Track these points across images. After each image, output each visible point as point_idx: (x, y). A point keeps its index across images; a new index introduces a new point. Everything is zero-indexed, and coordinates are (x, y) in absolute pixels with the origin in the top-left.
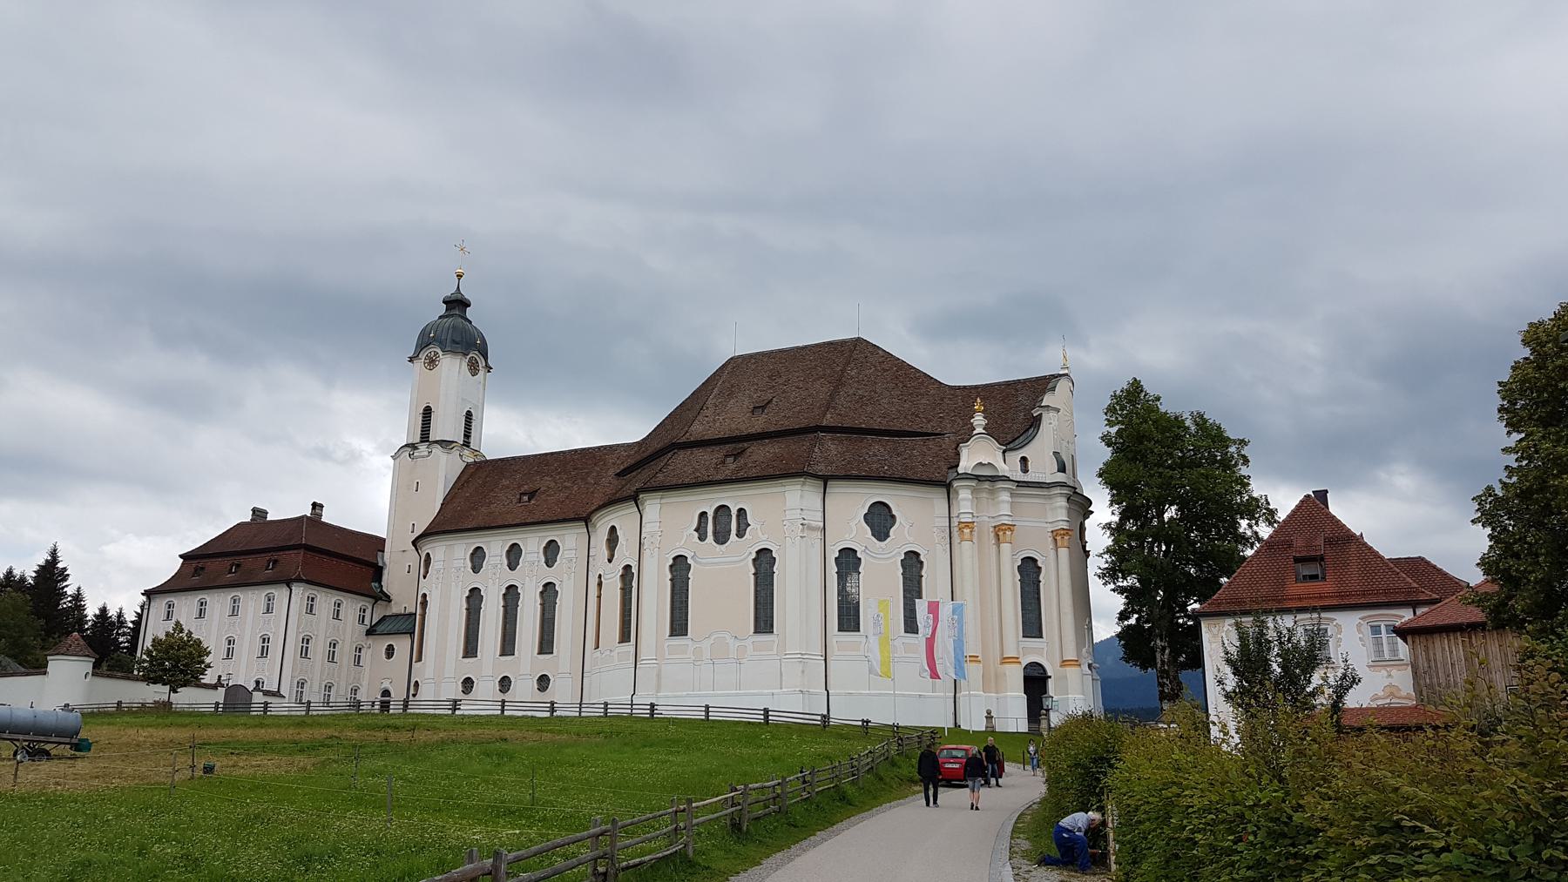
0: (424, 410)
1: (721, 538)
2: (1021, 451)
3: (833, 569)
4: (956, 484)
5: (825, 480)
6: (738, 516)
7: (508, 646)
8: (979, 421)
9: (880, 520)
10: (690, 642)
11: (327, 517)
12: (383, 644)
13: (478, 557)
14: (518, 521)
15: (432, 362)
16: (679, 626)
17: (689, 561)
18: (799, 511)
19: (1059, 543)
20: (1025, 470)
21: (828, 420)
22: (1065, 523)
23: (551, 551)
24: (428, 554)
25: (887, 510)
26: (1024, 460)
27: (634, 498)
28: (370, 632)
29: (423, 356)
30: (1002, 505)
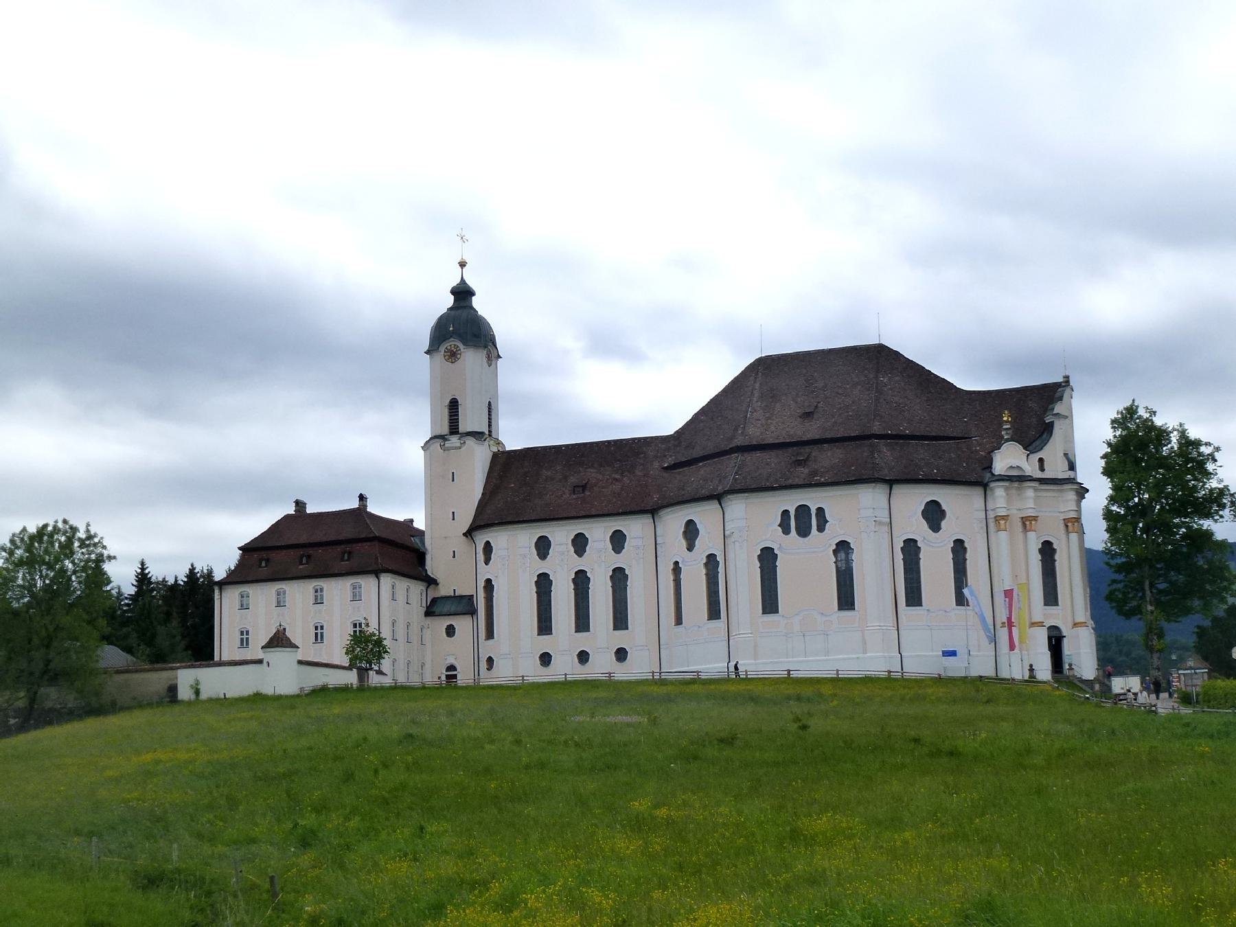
0: (450, 402)
1: (804, 531)
2: (1039, 453)
3: (899, 556)
4: (992, 485)
5: (891, 483)
6: (817, 515)
7: (582, 623)
9: (934, 515)
11: (373, 508)
12: (443, 623)
13: (543, 547)
14: (583, 513)
15: (453, 356)
16: (770, 604)
18: (872, 510)
19: (1070, 529)
20: (1042, 469)
21: (877, 428)
22: (1074, 513)
23: (618, 540)
24: (488, 544)
26: (1041, 460)
27: (718, 497)
28: (429, 613)
29: (442, 348)
30: (1029, 500)
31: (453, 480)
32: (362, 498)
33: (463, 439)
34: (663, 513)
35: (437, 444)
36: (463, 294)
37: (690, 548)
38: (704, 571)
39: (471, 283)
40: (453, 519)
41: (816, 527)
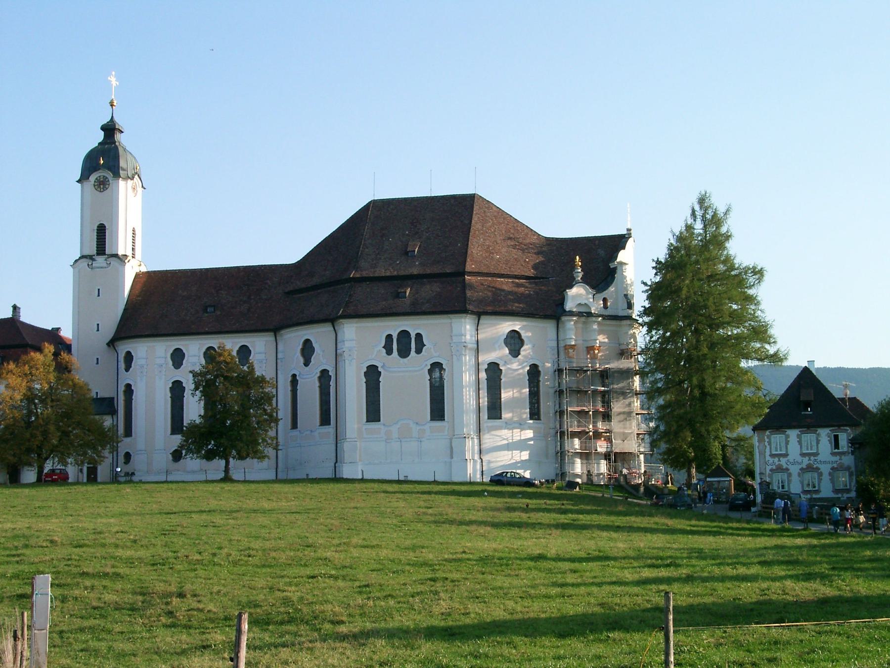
0: (98, 227)
1: (404, 352)
3: (483, 375)
5: (479, 315)
8: (579, 273)
10: (382, 427)
11: (26, 317)
13: (178, 357)
15: (102, 185)
16: (373, 414)
17: (380, 369)
25: (517, 336)
27: (332, 320)
29: (93, 178)
31: (99, 296)
32: (15, 308)
33: (109, 259)
34: (283, 332)
35: (84, 263)
36: (110, 130)
37: (307, 363)
38: (317, 384)
39: (120, 122)
40: (98, 330)
41: (414, 350)
